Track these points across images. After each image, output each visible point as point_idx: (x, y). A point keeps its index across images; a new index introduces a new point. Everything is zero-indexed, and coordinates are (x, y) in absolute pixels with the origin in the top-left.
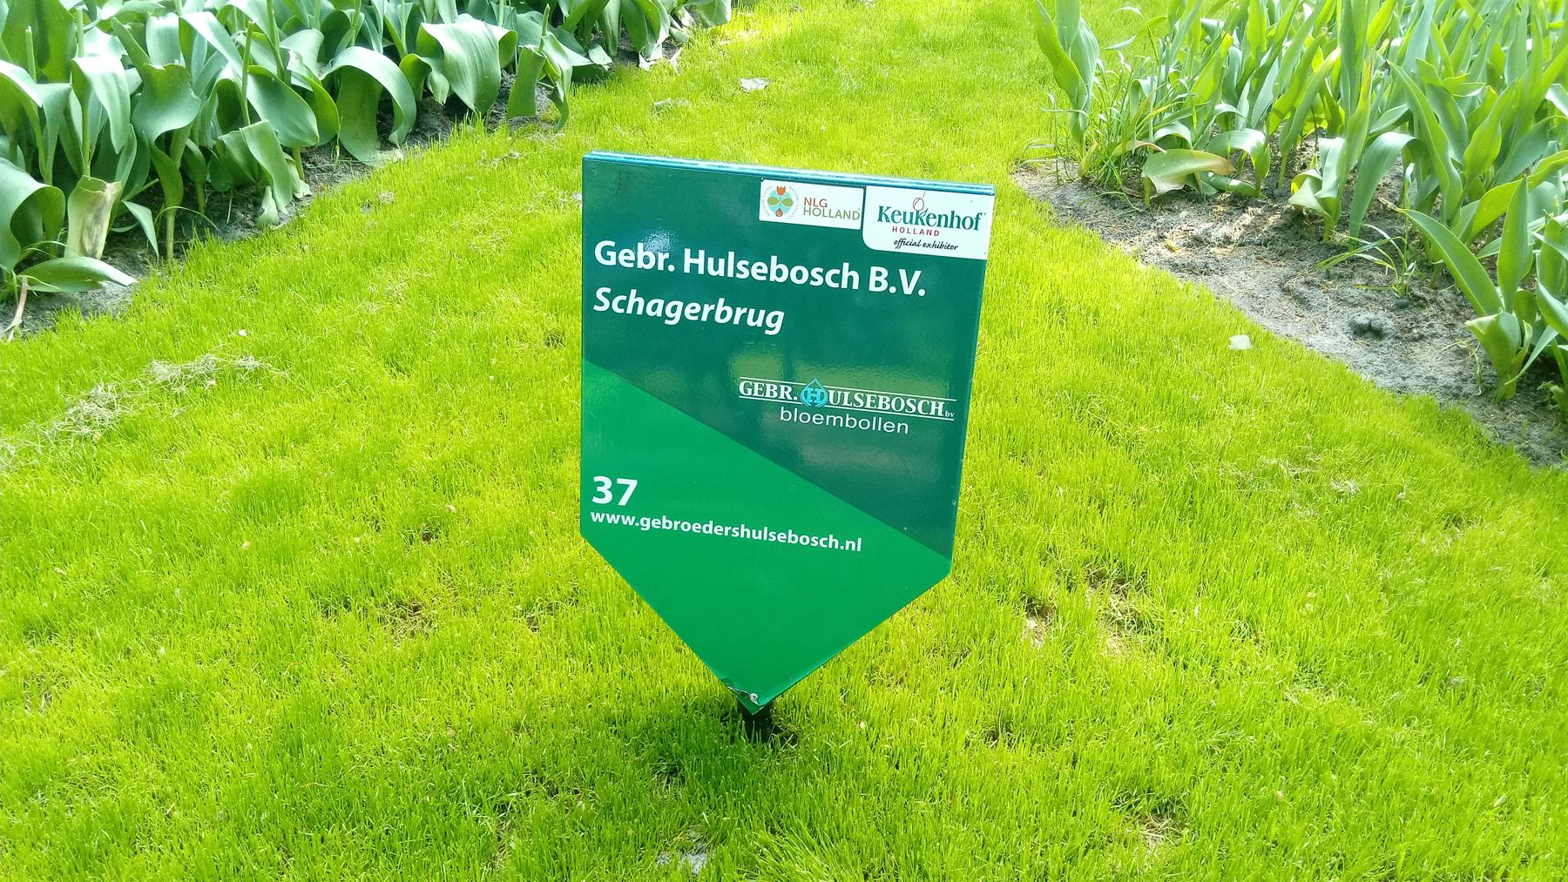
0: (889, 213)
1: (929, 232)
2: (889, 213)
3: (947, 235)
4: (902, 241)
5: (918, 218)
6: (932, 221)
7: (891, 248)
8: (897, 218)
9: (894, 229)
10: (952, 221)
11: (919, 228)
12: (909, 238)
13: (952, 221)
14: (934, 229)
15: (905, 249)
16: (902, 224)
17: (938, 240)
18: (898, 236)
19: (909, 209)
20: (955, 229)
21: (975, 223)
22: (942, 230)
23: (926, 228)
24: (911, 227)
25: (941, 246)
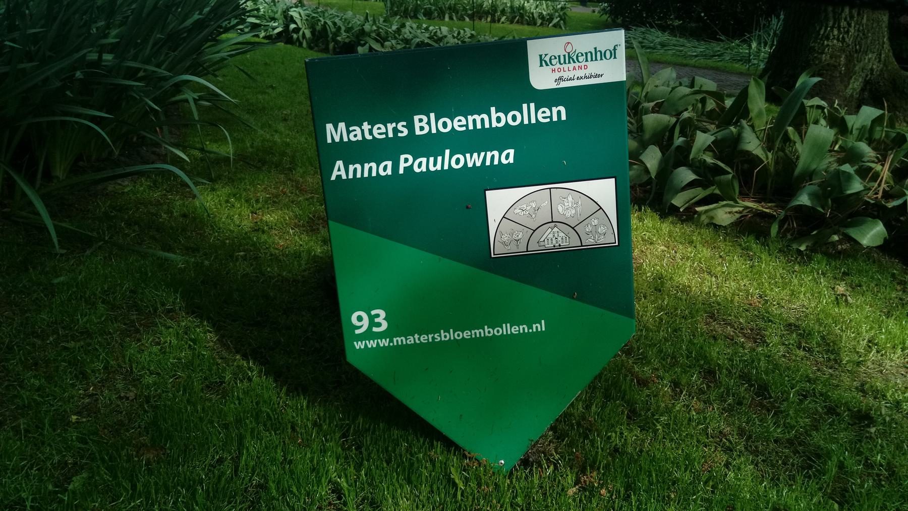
0: (547, 59)
1: (580, 68)
2: (547, 59)
3: (594, 67)
4: (561, 79)
5: (570, 58)
6: (581, 59)
7: (554, 86)
8: (554, 62)
9: (553, 71)
10: (596, 55)
11: (572, 65)
12: (565, 75)
15: (563, 85)
16: (558, 66)
17: (588, 72)
18: (557, 75)
20: (599, 62)
21: (613, 53)
22: (589, 64)
23: (577, 65)
24: (566, 66)
25: (591, 77)
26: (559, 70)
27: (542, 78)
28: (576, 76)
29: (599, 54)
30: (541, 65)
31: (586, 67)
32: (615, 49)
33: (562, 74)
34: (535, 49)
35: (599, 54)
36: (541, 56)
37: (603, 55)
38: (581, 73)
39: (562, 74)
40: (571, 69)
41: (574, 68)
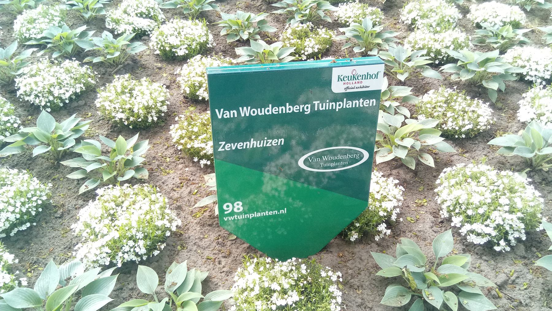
0: (342, 78)
1: (358, 82)
2: (342, 78)
3: (365, 83)
4: (348, 88)
6: (359, 78)
7: (344, 91)
8: (345, 79)
10: (368, 76)
11: (355, 81)
12: (350, 86)
13: (368, 76)
14: (360, 81)
15: (348, 91)
16: (347, 81)
17: (362, 85)
18: (346, 86)
19: (350, 75)
20: (369, 80)
21: (376, 76)
23: (357, 81)
24: (351, 82)
25: (363, 87)
26: (347, 83)
27: (337, 87)
28: (355, 87)
29: (369, 76)
30: (338, 81)
31: (361, 82)
32: (377, 74)
33: (349, 85)
34: (336, 73)
35: (369, 76)
36: (339, 76)
37: (371, 77)
38: (358, 85)
39: (349, 85)
40: (354, 83)
41: (355, 83)
